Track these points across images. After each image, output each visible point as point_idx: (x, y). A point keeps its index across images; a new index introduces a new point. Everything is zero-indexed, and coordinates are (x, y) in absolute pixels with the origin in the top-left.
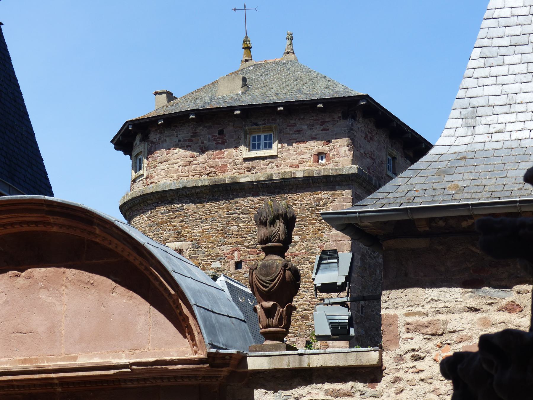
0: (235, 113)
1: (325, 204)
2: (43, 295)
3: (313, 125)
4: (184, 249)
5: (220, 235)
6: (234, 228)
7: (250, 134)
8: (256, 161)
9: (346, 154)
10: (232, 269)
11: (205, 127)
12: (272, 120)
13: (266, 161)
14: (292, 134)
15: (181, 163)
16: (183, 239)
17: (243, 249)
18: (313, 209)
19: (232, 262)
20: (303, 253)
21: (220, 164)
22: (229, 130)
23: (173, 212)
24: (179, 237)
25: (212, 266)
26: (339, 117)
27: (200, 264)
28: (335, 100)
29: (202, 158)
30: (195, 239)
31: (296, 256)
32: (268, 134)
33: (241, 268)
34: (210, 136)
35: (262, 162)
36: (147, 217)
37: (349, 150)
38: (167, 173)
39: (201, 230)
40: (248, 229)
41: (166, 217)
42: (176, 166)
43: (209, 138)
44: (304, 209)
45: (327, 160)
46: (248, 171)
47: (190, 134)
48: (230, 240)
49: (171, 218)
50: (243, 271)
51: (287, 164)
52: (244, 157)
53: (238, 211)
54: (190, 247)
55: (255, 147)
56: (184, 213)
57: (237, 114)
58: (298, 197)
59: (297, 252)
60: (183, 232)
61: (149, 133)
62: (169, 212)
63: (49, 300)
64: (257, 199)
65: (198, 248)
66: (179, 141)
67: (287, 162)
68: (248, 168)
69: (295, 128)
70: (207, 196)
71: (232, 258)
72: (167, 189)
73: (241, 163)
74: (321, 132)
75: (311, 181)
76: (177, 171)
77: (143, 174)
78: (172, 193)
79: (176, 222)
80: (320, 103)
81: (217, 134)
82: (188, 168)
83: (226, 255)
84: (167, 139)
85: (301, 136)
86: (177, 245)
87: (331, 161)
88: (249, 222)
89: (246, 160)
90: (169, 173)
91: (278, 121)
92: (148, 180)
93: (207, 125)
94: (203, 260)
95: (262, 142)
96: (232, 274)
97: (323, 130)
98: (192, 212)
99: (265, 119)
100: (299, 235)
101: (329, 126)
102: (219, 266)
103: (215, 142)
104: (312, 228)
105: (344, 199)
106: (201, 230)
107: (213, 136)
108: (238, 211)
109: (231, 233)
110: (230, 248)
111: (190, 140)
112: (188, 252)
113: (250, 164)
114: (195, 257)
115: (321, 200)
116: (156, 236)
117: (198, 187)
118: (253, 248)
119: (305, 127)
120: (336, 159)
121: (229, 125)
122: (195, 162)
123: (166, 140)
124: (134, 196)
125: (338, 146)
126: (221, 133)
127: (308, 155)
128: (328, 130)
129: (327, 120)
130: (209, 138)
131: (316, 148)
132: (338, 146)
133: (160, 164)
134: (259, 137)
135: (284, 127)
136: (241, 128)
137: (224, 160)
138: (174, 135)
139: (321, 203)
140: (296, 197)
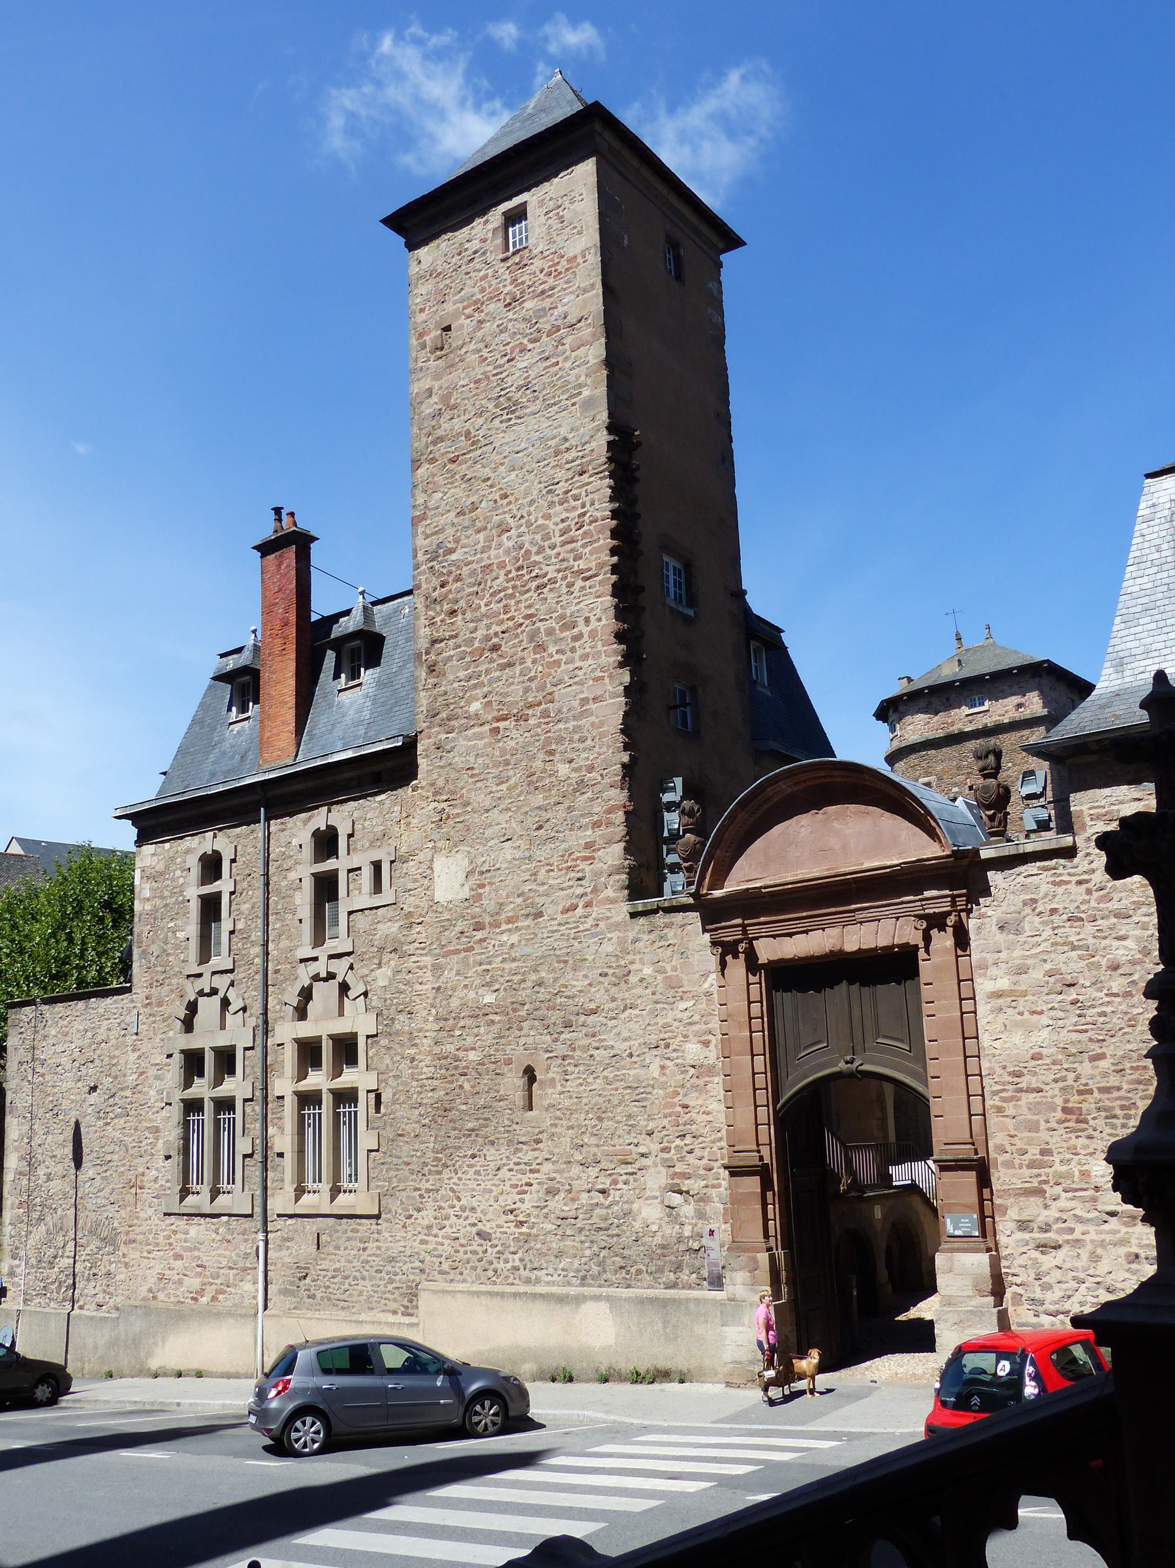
2: (836, 824)
6: (965, 763)
10: (967, 791)
19: (967, 786)
29: (938, 717)
55: (971, 707)
63: (840, 826)
64: (978, 741)
83: (961, 782)
89: (967, 715)
110: (964, 777)
126: (948, 699)
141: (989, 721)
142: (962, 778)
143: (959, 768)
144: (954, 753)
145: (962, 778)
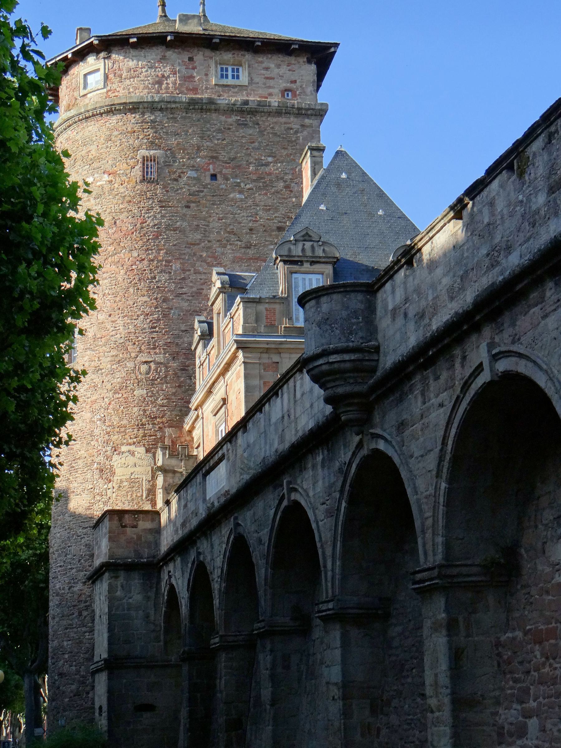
0: (214, 41)
1: (296, 132)
3: (280, 65)
7: (220, 64)
10: (208, 180)
11: (176, 52)
13: (236, 90)
14: (261, 70)
17: (218, 163)
18: (285, 136)
26: (304, 62)
28: (310, 44)
32: (235, 67)
33: (216, 180)
34: (180, 61)
44: (275, 134)
47: (159, 57)
50: (219, 182)
58: (270, 125)
62: (142, 122)
64: (230, 120)
67: (256, 92)
70: (180, 113)
75: (284, 111)
78: (146, 105)
80: (296, 44)
81: (187, 60)
85: (269, 72)
88: (223, 140)
91: (247, 56)
92: (110, 93)
93: (176, 50)
95: (230, 73)
96: (209, 184)
97: (289, 70)
100: (272, 157)
101: (295, 67)
103: (185, 67)
104: (284, 152)
105: (313, 131)
107: (183, 61)
115: (291, 129)
117: (175, 102)
119: (272, 66)
126: (191, 59)
128: (294, 71)
129: (293, 62)
130: (179, 63)
132: (304, 86)
134: (227, 70)
136: (211, 58)
140: (267, 124)
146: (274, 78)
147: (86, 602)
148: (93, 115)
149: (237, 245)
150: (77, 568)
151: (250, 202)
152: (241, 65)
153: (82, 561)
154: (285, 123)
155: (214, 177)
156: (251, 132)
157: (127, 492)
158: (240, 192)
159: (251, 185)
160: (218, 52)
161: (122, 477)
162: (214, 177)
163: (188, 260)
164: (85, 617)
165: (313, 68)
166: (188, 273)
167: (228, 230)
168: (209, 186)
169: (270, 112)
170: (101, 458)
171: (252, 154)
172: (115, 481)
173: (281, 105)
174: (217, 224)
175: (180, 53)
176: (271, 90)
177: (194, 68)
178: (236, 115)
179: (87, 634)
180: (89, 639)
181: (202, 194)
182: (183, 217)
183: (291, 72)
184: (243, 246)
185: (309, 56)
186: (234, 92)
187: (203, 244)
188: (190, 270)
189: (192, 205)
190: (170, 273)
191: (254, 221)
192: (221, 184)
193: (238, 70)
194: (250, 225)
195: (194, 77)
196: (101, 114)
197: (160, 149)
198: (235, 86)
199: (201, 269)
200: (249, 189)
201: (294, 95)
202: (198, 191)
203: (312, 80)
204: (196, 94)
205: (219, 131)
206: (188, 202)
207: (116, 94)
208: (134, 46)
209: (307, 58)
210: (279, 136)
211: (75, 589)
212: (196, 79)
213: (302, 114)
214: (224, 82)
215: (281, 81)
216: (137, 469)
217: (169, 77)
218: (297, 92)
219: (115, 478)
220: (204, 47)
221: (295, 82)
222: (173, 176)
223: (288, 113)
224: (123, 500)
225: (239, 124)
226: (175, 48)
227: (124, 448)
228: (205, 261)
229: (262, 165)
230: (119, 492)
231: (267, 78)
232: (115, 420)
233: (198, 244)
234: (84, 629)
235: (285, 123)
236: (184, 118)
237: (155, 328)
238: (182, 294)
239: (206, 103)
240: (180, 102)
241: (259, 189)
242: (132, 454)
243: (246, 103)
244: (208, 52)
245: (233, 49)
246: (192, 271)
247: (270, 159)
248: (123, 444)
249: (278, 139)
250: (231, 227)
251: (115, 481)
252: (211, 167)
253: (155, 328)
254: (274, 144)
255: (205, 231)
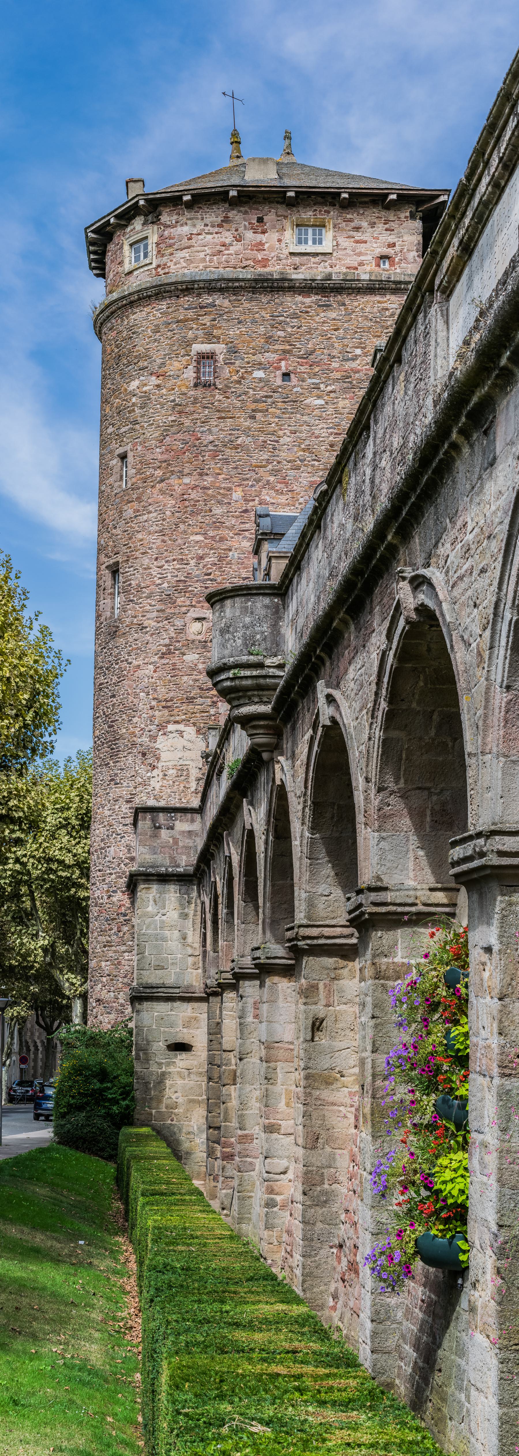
3: (375, 223)
4: (217, 352)
5: (263, 340)
6: (281, 333)
8: (305, 258)
9: (415, 260)
10: (279, 381)
11: (239, 211)
12: (325, 211)
14: (349, 231)
15: (208, 252)
16: (215, 340)
18: (378, 320)
19: (279, 373)
20: (366, 369)
21: (260, 257)
22: (270, 218)
23: (201, 308)
24: (210, 337)
25: (254, 375)
26: (406, 217)
27: (238, 371)
30: (232, 342)
31: (358, 371)
33: (289, 381)
34: (247, 223)
35: (313, 260)
36: (161, 313)
37: (418, 256)
38: (189, 261)
39: (238, 332)
40: (298, 336)
41: (191, 314)
42: (202, 255)
43: (245, 225)
45: (391, 265)
46: (295, 269)
47: (219, 219)
48: (276, 347)
49: (199, 315)
50: (293, 384)
51: (344, 265)
52: (291, 251)
53: (285, 314)
54: (225, 351)
56: (216, 310)
57: (290, 197)
58: (359, 305)
59: (359, 367)
60: (215, 332)
61: (160, 214)
62: (196, 308)
64: (308, 300)
65: (235, 352)
66: (206, 225)
68: (295, 264)
69: (353, 224)
71: (279, 368)
72: (197, 278)
73: (287, 258)
74: (384, 232)
76: (204, 260)
77: (151, 263)
79: (206, 320)
81: (255, 221)
82: (218, 259)
84: (189, 222)
85: (360, 234)
86: (205, 348)
87: (397, 266)
88: (299, 328)
89: (292, 254)
90: (192, 262)
91: (332, 213)
92: (159, 270)
93: (242, 209)
94: (242, 368)
96: (280, 387)
97: (387, 230)
98: (227, 310)
99: (316, 210)
100: (362, 348)
102: (264, 376)
106: (238, 332)
107: (250, 223)
108: (285, 314)
109: (276, 338)
111: (220, 226)
112: (222, 357)
113: (297, 260)
114: (231, 363)
115: (387, 309)
116: (177, 336)
117: (237, 280)
118: (304, 358)
119: (365, 224)
120: (403, 265)
121: (270, 211)
122: (227, 252)
123: (186, 224)
124: (143, 287)
125: (405, 250)
126: (260, 220)
127: (370, 258)
130: (245, 225)
131: (380, 250)
132: (405, 250)
133: (179, 251)
135: (339, 221)
136: (286, 217)
137: (265, 252)
138: (197, 219)
139: (387, 313)
140: (356, 304)
141: (338, 270)
142: (271, 357)
143: (269, 339)
144: (263, 313)
145: (271, 357)
146: (366, 242)
147: (125, 915)
148: (140, 299)
149: (313, 466)
150: (115, 873)
151: (330, 410)
152: (324, 226)
153: (122, 865)
154: (379, 302)
155: (286, 375)
156: (333, 315)
157: (174, 782)
158: (319, 397)
159: (333, 387)
160: (294, 209)
161: (168, 764)
162: (286, 375)
163: (252, 486)
164: (124, 934)
165: (418, 224)
166: (251, 504)
167: (303, 446)
168: (280, 390)
169: (360, 288)
170: (145, 739)
171: (336, 345)
172: (160, 768)
173: (373, 278)
174: (289, 439)
175: (246, 213)
176: (362, 258)
177: (264, 232)
178: (317, 294)
179: (127, 954)
180: (128, 960)
181: (269, 400)
182: (247, 431)
183: (389, 232)
184: (322, 467)
185: (414, 209)
186: (314, 263)
187: (270, 467)
188: (254, 500)
189: (259, 415)
190: (230, 503)
191: (336, 434)
192: (295, 386)
193: (320, 234)
194: (331, 438)
195: (263, 245)
196: (149, 297)
197: (219, 343)
198: (316, 254)
199: (268, 499)
200: (331, 392)
201: (392, 264)
202: (266, 397)
203: (416, 242)
204: (265, 266)
205: (294, 316)
206: (253, 411)
207: (167, 270)
208: (189, 205)
209: (411, 212)
210: (371, 320)
211: (114, 899)
212: (266, 246)
213: (400, 289)
214: (302, 249)
215: (375, 245)
216: (187, 754)
217: (231, 245)
218: (397, 260)
219: (160, 765)
220: (278, 202)
221: (393, 245)
222: (235, 378)
223: (383, 289)
224: (169, 791)
225: (319, 306)
226: (241, 206)
227: (171, 727)
228: (273, 488)
229: (348, 360)
230: (165, 782)
231: (357, 242)
232: (162, 692)
233: (265, 466)
234: (124, 948)
235: (379, 302)
236: (251, 300)
237: (210, 574)
238: (243, 531)
239: (277, 280)
240: (243, 280)
241: (345, 390)
242: (181, 733)
243: (328, 277)
244: (282, 210)
245: (315, 204)
246: (257, 502)
247: (358, 352)
248: (168, 722)
249: (370, 324)
250: (307, 442)
251: (160, 768)
252: (283, 363)
253: (210, 574)
254: (364, 332)
255: (275, 449)
